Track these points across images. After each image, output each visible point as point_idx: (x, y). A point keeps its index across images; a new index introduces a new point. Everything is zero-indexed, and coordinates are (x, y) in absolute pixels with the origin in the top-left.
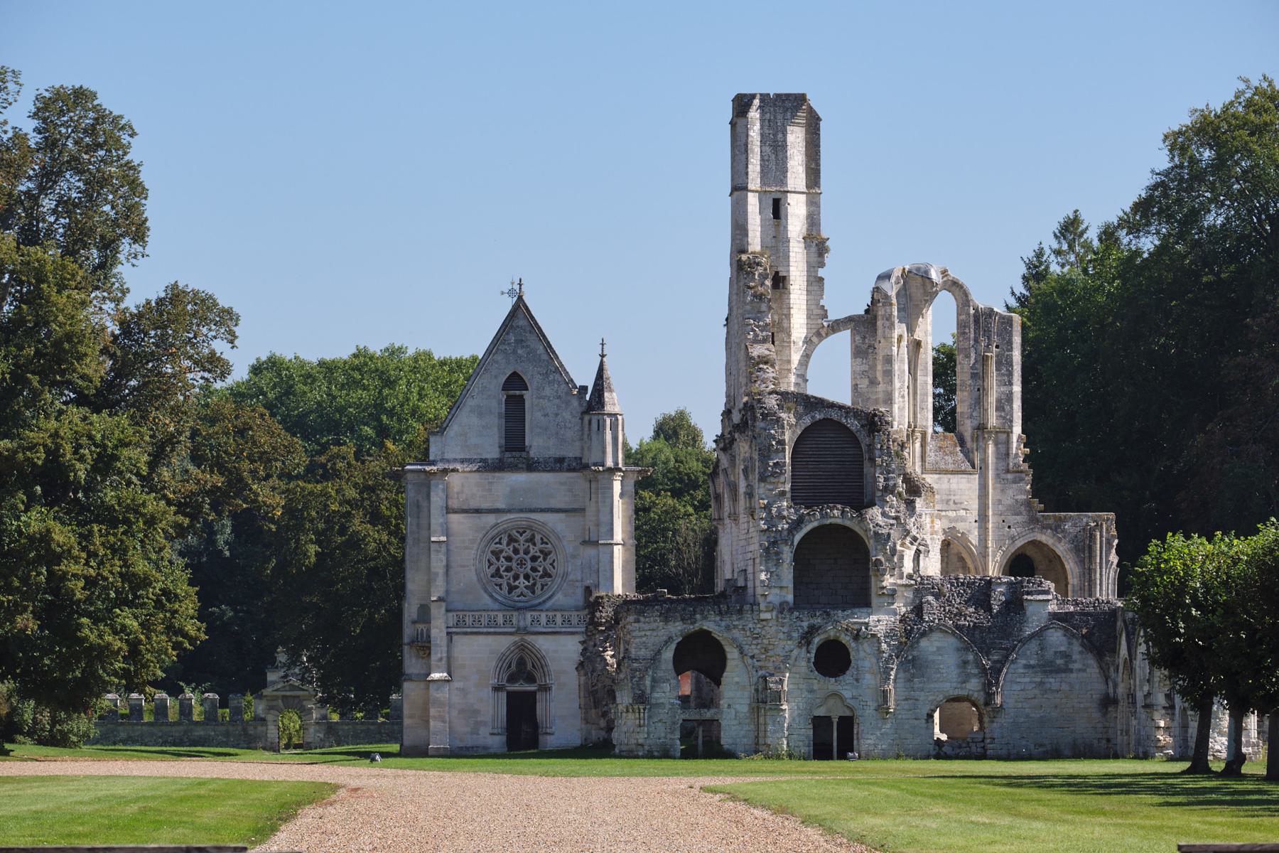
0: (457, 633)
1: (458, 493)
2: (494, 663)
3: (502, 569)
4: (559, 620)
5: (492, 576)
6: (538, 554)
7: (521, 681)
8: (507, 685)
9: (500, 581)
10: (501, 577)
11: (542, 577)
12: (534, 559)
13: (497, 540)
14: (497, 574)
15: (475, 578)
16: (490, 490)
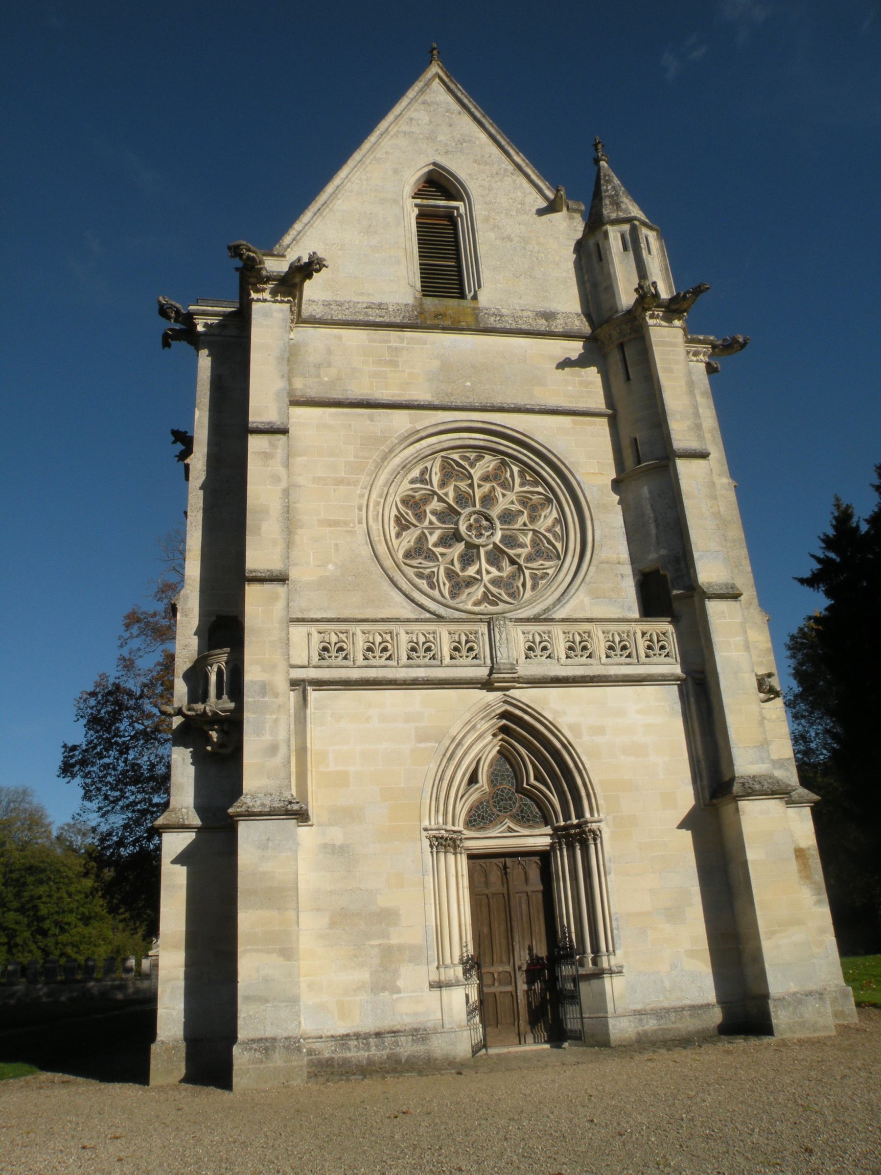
0: (319, 684)
1: (318, 366)
2: (433, 766)
3: (433, 539)
4: (599, 645)
5: (408, 555)
6: (517, 507)
7: (509, 823)
8: (468, 833)
9: (429, 566)
10: (431, 556)
11: (529, 558)
12: (508, 517)
13: (416, 473)
14: (419, 550)
15: (367, 551)
16: (394, 364)
